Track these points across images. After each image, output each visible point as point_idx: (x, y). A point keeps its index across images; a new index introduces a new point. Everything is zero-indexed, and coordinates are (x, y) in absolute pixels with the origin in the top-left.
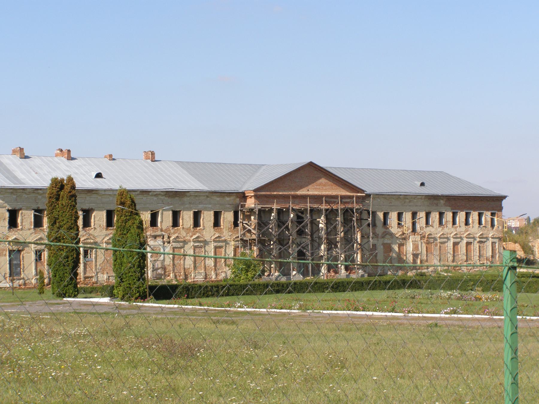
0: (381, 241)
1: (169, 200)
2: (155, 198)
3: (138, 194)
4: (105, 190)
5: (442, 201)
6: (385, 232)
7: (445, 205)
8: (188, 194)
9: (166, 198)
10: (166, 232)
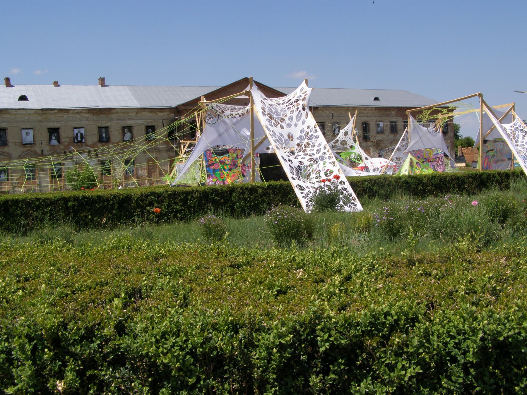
1: (94, 117)
2: (78, 116)
3: (56, 113)
4: (16, 110)
5: (393, 112)
7: (396, 115)
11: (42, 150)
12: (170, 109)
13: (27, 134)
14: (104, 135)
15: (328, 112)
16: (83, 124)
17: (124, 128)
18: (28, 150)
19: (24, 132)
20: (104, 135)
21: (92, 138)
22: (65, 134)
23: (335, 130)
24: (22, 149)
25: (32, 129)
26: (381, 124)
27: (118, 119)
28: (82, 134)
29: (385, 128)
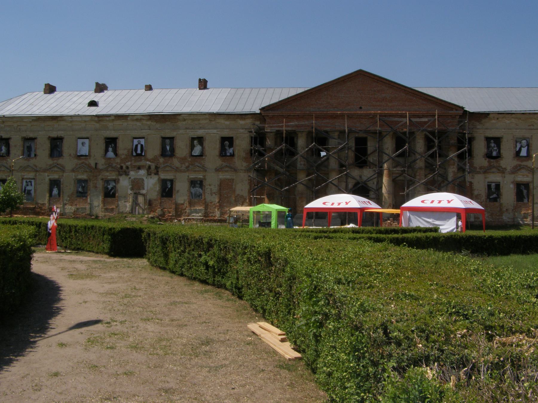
0: (509, 178)
1: (158, 126)
2: (138, 124)
3: (113, 120)
6: (520, 165)
8: (180, 118)
9: (154, 123)
10: (152, 162)
11: (96, 164)
12: (253, 115)
13: (83, 144)
14: (168, 148)
15: (508, 122)
16: (144, 133)
17: (193, 139)
18: (83, 163)
19: (80, 141)
20: (168, 148)
21: (153, 151)
22: (123, 146)
23: (520, 150)
24: (76, 161)
27: (187, 128)
28: (142, 146)
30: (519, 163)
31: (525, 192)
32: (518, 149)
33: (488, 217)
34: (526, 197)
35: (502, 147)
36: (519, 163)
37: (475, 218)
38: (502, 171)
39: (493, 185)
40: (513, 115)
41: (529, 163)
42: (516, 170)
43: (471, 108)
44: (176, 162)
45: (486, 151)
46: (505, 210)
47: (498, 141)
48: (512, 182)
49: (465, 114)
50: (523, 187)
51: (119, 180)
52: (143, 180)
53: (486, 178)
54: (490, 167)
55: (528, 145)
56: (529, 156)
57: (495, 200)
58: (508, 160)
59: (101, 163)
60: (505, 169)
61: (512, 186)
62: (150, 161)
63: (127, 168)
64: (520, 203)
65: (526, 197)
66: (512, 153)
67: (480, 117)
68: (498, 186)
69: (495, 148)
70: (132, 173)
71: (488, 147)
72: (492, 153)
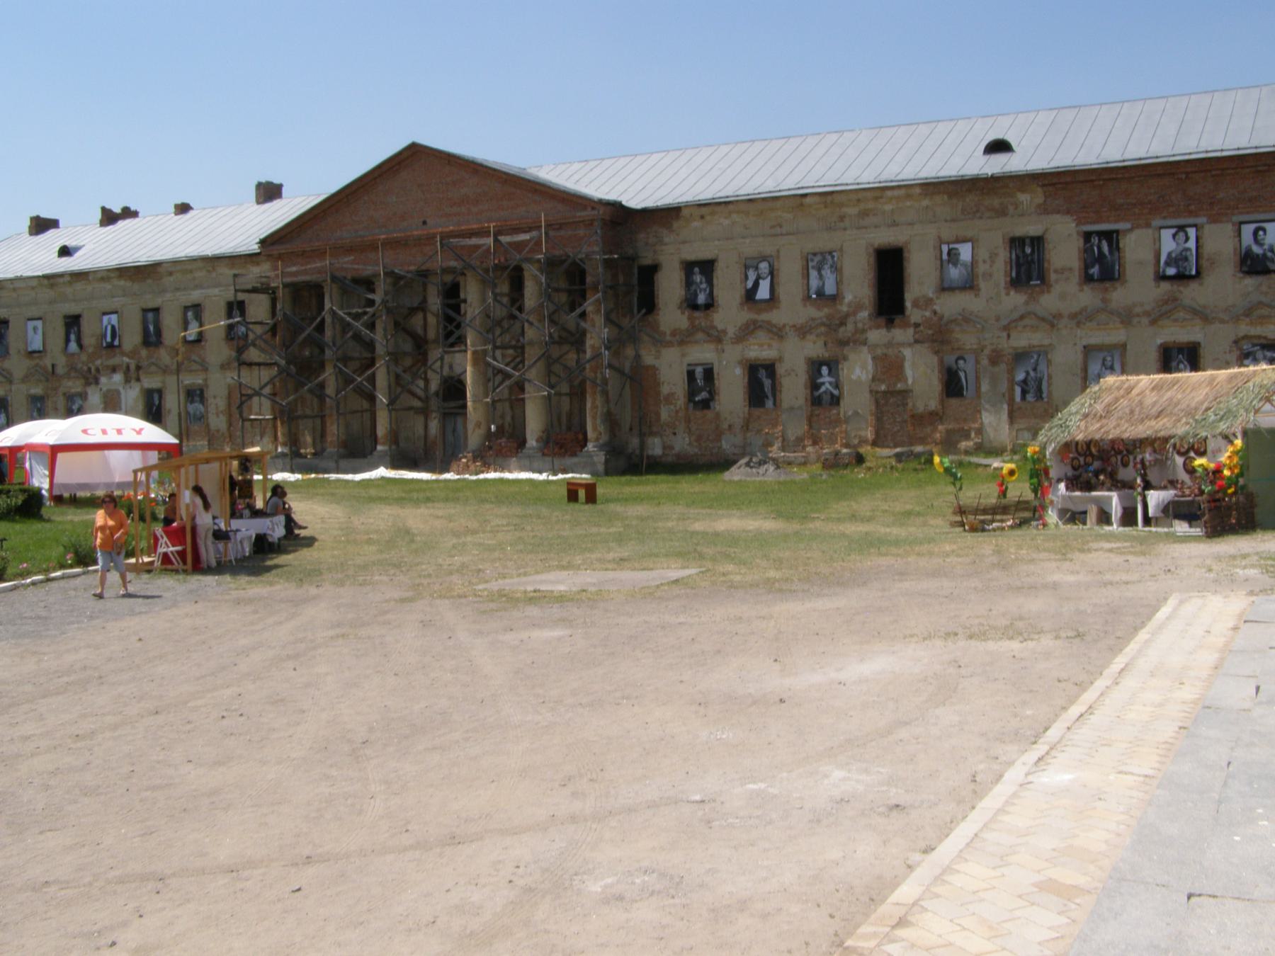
5: (1024, 198)
6: (755, 322)
7: (1044, 210)
11: (53, 366)
13: (35, 329)
14: (151, 328)
15: (726, 222)
16: (116, 302)
17: (186, 308)
18: (37, 365)
19: (31, 324)
20: (151, 328)
21: (132, 338)
22: (89, 328)
23: (756, 285)
24: (28, 363)
25: (40, 319)
26: (965, 252)
27: (178, 289)
28: (113, 327)
29: (981, 268)
30: (754, 316)
31: (767, 383)
32: (750, 284)
33: (690, 444)
34: (769, 395)
35: (715, 281)
36: (754, 316)
37: (664, 448)
38: (717, 338)
39: (699, 370)
40: (731, 207)
41: (777, 317)
42: (748, 330)
43: (634, 201)
44: (164, 356)
45: (683, 293)
46: (725, 426)
47: (707, 267)
48: (740, 363)
49: (619, 218)
50: (762, 374)
51: (86, 394)
52: (118, 392)
53: (683, 355)
54: (694, 329)
55: (772, 273)
56: (773, 299)
57: (706, 404)
58: (729, 314)
59: (61, 361)
60: (724, 332)
61: (738, 371)
62: (127, 356)
63: (98, 370)
64: (757, 412)
65: (769, 395)
66: (738, 294)
67: (666, 216)
68: (709, 373)
69: (704, 286)
70: (103, 380)
71: (689, 283)
72: (696, 295)
